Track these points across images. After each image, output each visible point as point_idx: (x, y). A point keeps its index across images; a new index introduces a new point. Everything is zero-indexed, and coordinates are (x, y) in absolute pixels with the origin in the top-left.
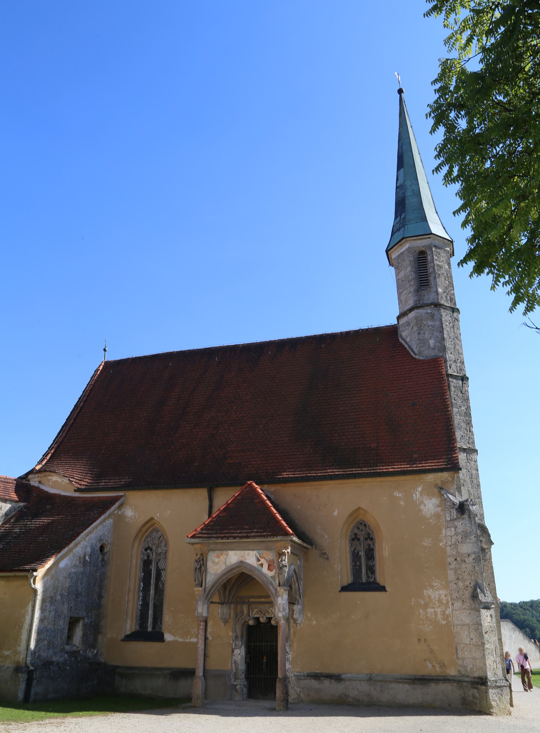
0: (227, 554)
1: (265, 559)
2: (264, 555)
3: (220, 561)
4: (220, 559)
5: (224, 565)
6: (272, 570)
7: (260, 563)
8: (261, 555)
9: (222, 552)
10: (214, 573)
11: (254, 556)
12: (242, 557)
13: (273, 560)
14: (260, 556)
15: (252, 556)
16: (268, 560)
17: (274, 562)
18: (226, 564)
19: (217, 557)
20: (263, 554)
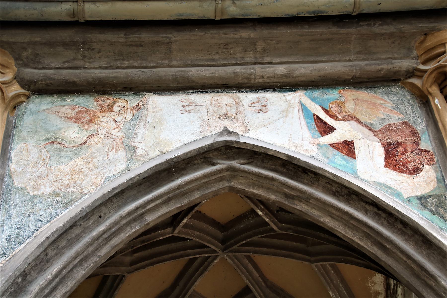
0: (138, 108)
1: (358, 121)
2: (350, 107)
3: (95, 139)
4: (93, 127)
5: (122, 154)
6: (416, 171)
7: (332, 138)
8: (334, 109)
9: (108, 100)
10: (53, 194)
11: (296, 111)
12: (226, 116)
13: (404, 123)
14: (327, 112)
15: (286, 112)
16: (379, 126)
17: (414, 133)
18: (131, 149)
19: (77, 119)
20: (340, 104)
